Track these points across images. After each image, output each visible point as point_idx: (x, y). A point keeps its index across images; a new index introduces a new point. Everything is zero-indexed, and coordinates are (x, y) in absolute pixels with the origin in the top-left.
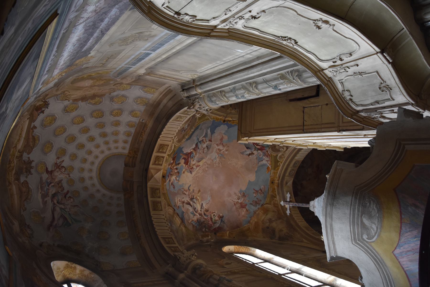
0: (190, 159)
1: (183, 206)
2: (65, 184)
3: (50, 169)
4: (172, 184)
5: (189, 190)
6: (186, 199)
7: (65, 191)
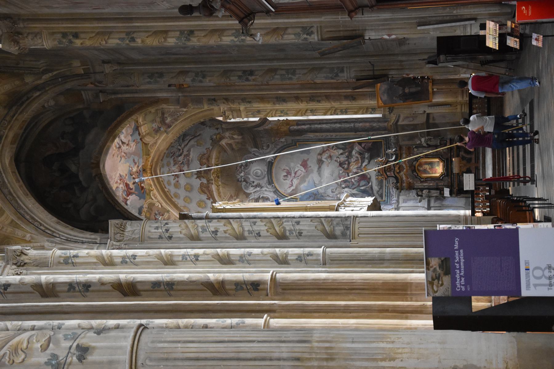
0: (126, 189)
1: (129, 141)
2: (172, 162)
4: (136, 163)
5: (121, 157)
6: (124, 148)
7: (173, 158)
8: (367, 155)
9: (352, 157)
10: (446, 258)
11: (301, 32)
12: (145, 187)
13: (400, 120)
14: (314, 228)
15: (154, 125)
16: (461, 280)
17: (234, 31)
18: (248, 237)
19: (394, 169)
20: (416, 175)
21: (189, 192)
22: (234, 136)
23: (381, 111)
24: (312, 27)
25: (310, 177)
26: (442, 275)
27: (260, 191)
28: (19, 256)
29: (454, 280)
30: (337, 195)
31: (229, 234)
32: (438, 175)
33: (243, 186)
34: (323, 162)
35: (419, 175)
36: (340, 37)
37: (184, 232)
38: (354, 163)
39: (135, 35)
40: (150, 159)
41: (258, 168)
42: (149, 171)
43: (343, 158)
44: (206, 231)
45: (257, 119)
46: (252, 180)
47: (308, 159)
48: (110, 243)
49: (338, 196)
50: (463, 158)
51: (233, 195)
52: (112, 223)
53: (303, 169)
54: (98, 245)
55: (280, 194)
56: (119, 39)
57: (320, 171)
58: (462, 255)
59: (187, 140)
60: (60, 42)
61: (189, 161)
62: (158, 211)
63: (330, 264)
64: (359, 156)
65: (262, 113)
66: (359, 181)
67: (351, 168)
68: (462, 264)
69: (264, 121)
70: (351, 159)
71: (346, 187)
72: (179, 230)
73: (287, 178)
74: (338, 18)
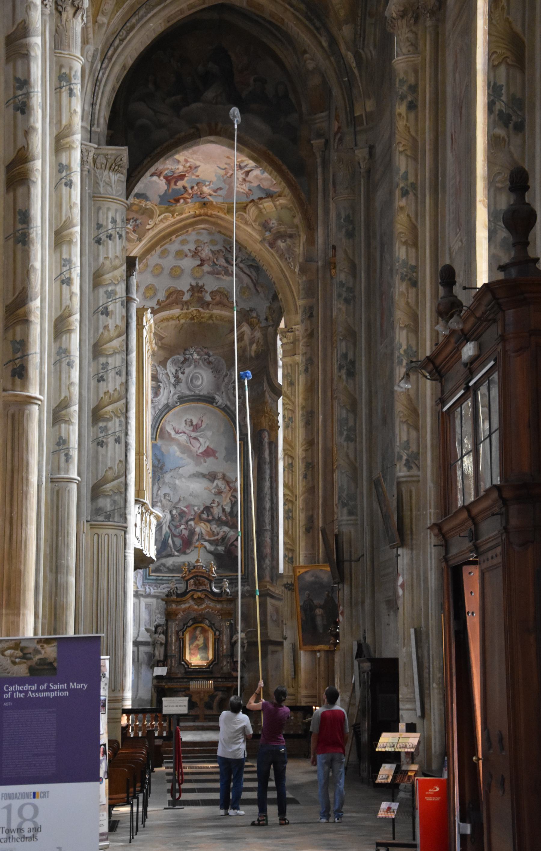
0: (175, 175)
1: (251, 182)
3: (199, 262)
4: (215, 191)
5: (225, 169)
7: (224, 249)
8: (221, 549)
9: (218, 526)
10: (55, 669)
11: (410, 450)
12: (178, 204)
13: (274, 601)
14: (109, 465)
15: (274, 221)
16: (21, 692)
17: (414, 349)
18: (98, 363)
19: (198, 591)
20: (189, 625)
21: (170, 273)
22: (255, 345)
23: (288, 572)
24: (418, 467)
25: (189, 460)
26: (29, 663)
27: (170, 383)
28: (73, 4)
29: (21, 681)
30: (161, 501)
31: (102, 333)
32: (188, 658)
33: (178, 356)
34: (213, 482)
35: (189, 629)
36: (402, 511)
37: (108, 263)
38: (209, 529)
39: (411, 196)
40: (221, 214)
41: (205, 380)
42: (202, 211)
43: (217, 511)
44: (108, 298)
45: (280, 380)
46: (187, 371)
47: (217, 458)
48: (91, 147)
49: (159, 504)
50: (212, 697)
51: (163, 341)
52: (123, 152)
53: (201, 450)
54: (89, 128)
55: (164, 413)
56: (406, 173)
57: (198, 477)
58: (60, 694)
59: (251, 272)
60: (402, 82)
61: (217, 274)
62: (141, 223)
63: (52, 489)
64: (219, 537)
65: (290, 389)
66: (181, 536)
67: (202, 524)
68: (47, 694)
69: (277, 392)
70: (216, 524)
71: (172, 516)
72: (110, 256)
73: (187, 426)
74: (430, 508)
